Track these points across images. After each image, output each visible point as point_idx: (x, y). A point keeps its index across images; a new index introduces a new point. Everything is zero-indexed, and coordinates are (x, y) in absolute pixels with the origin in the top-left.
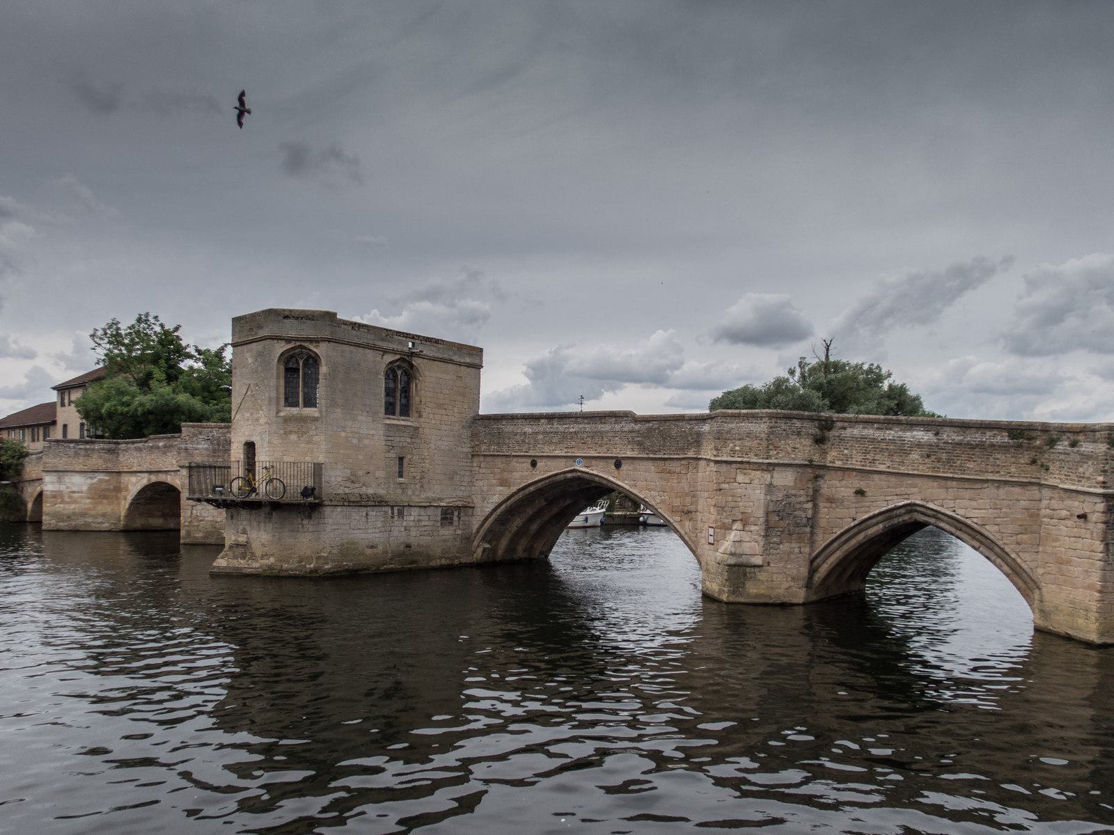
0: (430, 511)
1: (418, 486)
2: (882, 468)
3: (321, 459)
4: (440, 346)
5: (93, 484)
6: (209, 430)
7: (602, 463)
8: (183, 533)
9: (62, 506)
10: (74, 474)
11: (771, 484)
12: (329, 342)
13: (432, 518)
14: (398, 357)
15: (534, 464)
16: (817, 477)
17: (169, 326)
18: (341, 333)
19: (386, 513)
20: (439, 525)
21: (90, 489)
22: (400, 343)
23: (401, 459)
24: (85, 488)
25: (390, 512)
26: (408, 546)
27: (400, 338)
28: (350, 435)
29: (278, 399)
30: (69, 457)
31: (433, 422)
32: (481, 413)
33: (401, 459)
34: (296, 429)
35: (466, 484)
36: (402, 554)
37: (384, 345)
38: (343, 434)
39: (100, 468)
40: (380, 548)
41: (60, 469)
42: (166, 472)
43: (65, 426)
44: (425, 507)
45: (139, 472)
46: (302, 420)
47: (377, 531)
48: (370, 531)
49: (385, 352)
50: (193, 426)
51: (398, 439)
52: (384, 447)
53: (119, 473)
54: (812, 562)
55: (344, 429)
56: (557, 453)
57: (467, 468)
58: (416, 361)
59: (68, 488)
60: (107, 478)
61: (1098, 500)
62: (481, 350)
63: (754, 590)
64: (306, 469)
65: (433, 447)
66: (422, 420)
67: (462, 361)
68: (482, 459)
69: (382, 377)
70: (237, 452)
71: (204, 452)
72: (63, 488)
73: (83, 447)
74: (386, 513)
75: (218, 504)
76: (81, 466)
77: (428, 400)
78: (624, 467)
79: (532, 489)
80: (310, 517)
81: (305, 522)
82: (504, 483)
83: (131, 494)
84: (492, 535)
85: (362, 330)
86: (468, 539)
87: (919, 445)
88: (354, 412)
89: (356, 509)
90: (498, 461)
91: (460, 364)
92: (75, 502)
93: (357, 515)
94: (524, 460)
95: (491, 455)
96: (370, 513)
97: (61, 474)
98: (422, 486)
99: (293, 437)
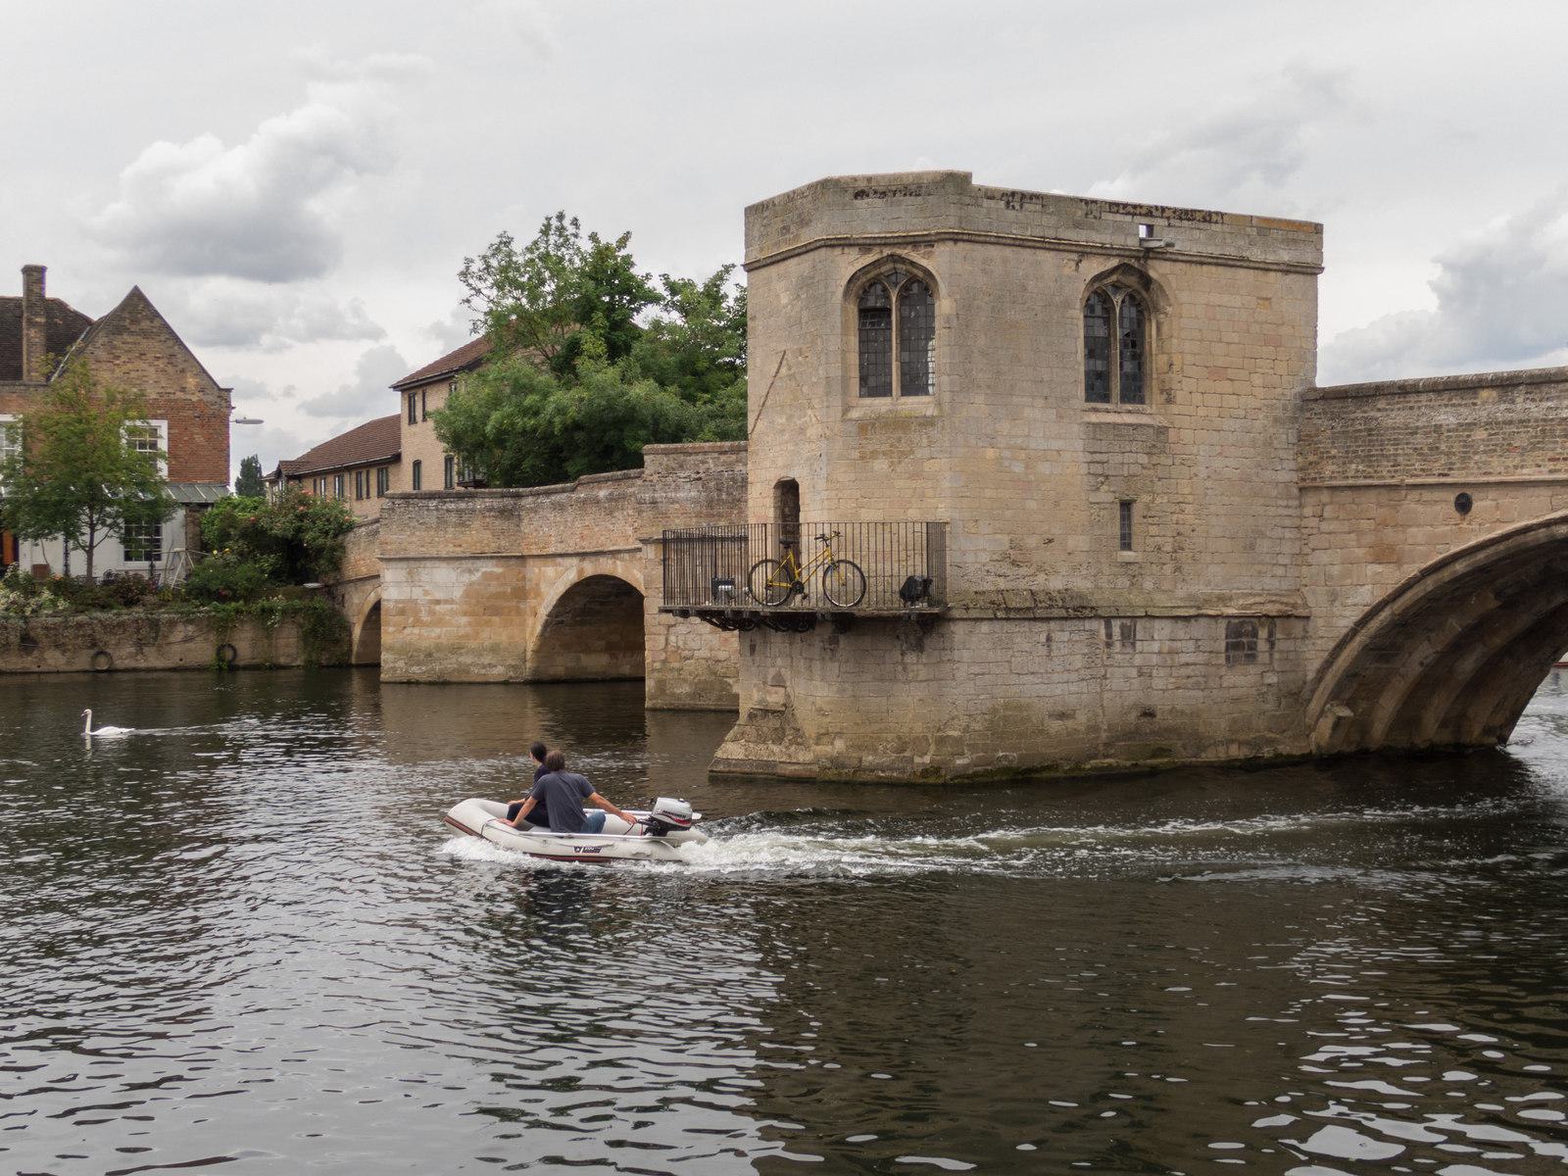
0: (1198, 628)
1: (1168, 569)
3: (942, 513)
4: (1214, 227)
5: (471, 584)
6: (700, 457)
8: (650, 685)
9: (416, 631)
10: (437, 563)
12: (956, 241)
13: (1205, 645)
14: (1114, 262)
15: (1464, 505)
17: (609, 238)
18: (982, 219)
19: (1093, 634)
20: (1222, 660)
21: (467, 594)
22: (1119, 228)
23: (1126, 505)
24: (458, 594)
25: (1103, 631)
26: (1148, 714)
27: (1119, 217)
28: (1007, 454)
29: (845, 380)
30: (428, 529)
31: (1202, 412)
32: (1324, 380)
33: (1126, 505)
34: (885, 447)
35: (1286, 561)
36: (1130, 734)
37: (1082, 237)
38: (990, 453)
39: (486, 549)
40: (1082, 718)
41: (412, 555)
42: (614, 553)
43: (417, 464)
44: (1186, 618)
45: (561, 555)
46: (899, 424)
47: (1074, 676)
48: (1055, 677)
49: (1083, 252)
50: (666, 453)
51: (1119, 458)
52: (1086, 479)
53: (522, 558)
55: (991, 440)
56: (1527, 474)
57: (1287, 522)
58: (1157, 270)
59: (426, 593)
60: (499, 570)
62: (1318, 229)
64: (910, 536)
65: (1204, 473)
66: (1175, 409)
67: (1271, 258)
68: (1325, 497)
69: (1078, 314)
70: (761, 506)
71: (690, 507)
72: (417, 593)
73: (452, 506)
74: (1093, 634)
75: (722, 620)
76: (451, 548)
77: (1189, 359)
79: (1460, 567)
80: (919, 647)
81: (910, 658)
82: (1384, 554)
83: (545, 604)
84: (1356, 686)
85: (1031, 207)
86: (1295, 696)
88: (1015, 400)
89: (1025, 626)
90: (1369, 500)
91: (1266, 269)
92: (439, 622)
93: (1026, 638)
94: (1437, 495)
96: (1057, 636)
97: (412, 564)
98: (1178, 569)
99: (880, 465)
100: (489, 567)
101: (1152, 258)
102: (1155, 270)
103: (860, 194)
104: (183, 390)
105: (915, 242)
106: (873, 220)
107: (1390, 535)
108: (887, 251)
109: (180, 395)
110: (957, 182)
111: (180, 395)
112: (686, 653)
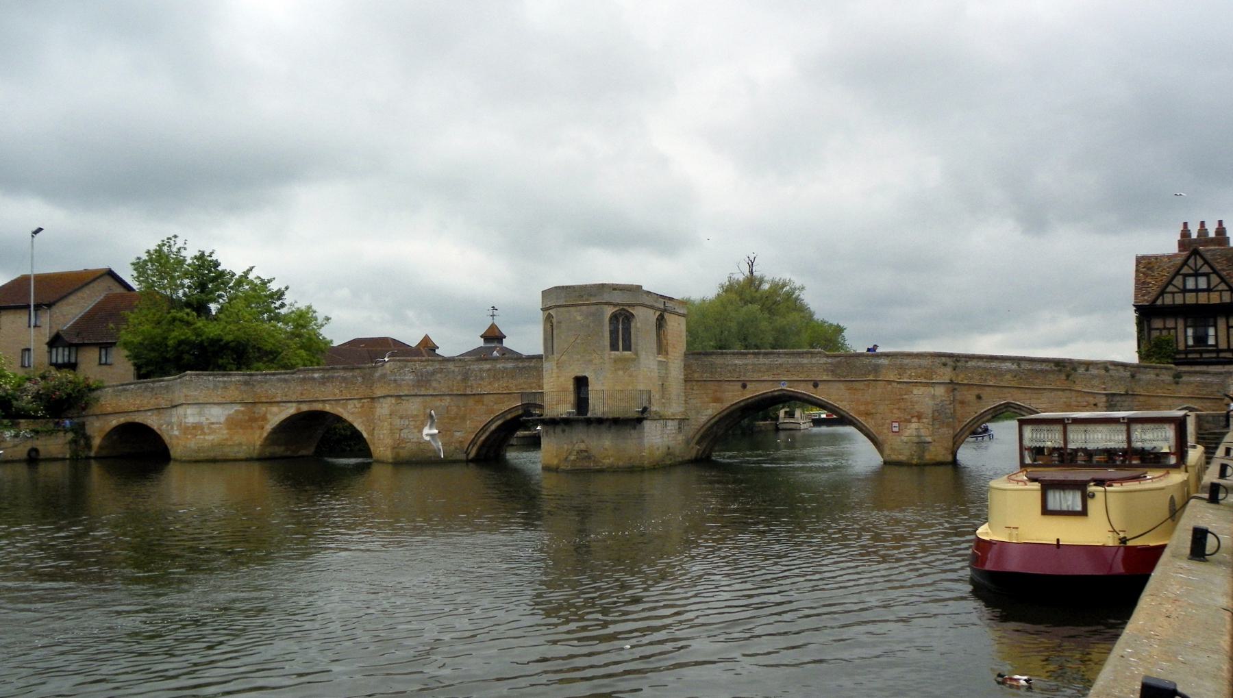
2: (991, 383)
5: (229, 415)
6: (413, 363)
7: (803, 385)
9: (202, 437)
10: (212, 405)
11: (934, 395)
15: (744, 386)
16: (955, 389)
21: (227, 419)
24: (222, 419)
30: (208, 390)
41: (201, 402)
42: (324, 401)
46: (626, 360)
50: (399, 361)
54: (954, 438)
56: (765, 378)
58: (666, 315)
59: (207, 419)
60: (243, 409)
61: (1104, 396)
63: (928, 457)
71: (410, 383)
72: (203, 419)
73: (221, 379)
78: (820, 387)
80: (635, 428)
81: (632, 431)
82: (717, 400)
83: (271, 423)
87: (1010, 371)
92: (213, 432)
94: (737, 383)
95: (803, 381)
97: (202, 406)
100: (238, 407)
103: (615, 289)
105: (630, 305)
106: (618, 298)
107: (718, 394)
108: (621, 307)
110: (639, 287)
112: (408, 440)
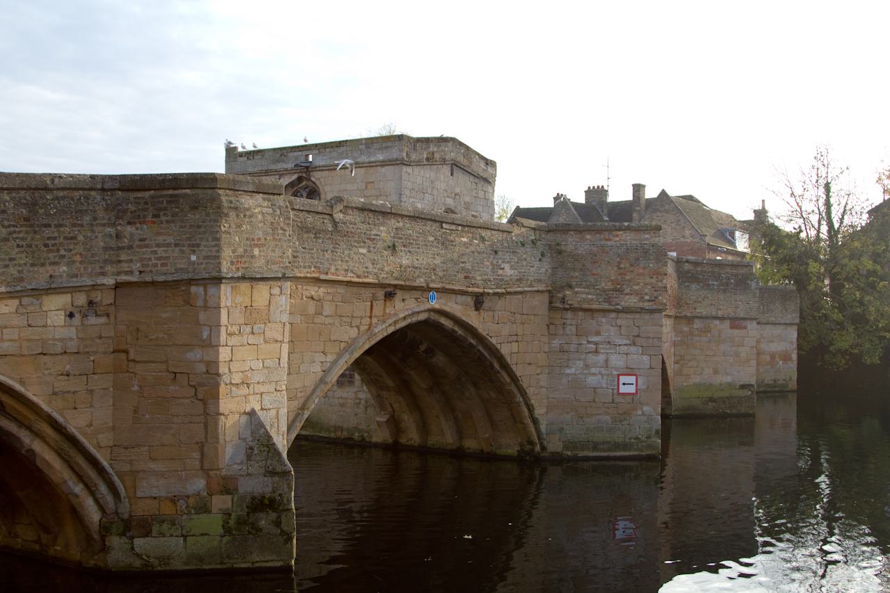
14: (295, 177)
27: (296, 154)
67: (373, 159)
101: (312, 171)
102: (314, 177)
104: (684, 237)
109: (682, 239)
111: (682, 239)
